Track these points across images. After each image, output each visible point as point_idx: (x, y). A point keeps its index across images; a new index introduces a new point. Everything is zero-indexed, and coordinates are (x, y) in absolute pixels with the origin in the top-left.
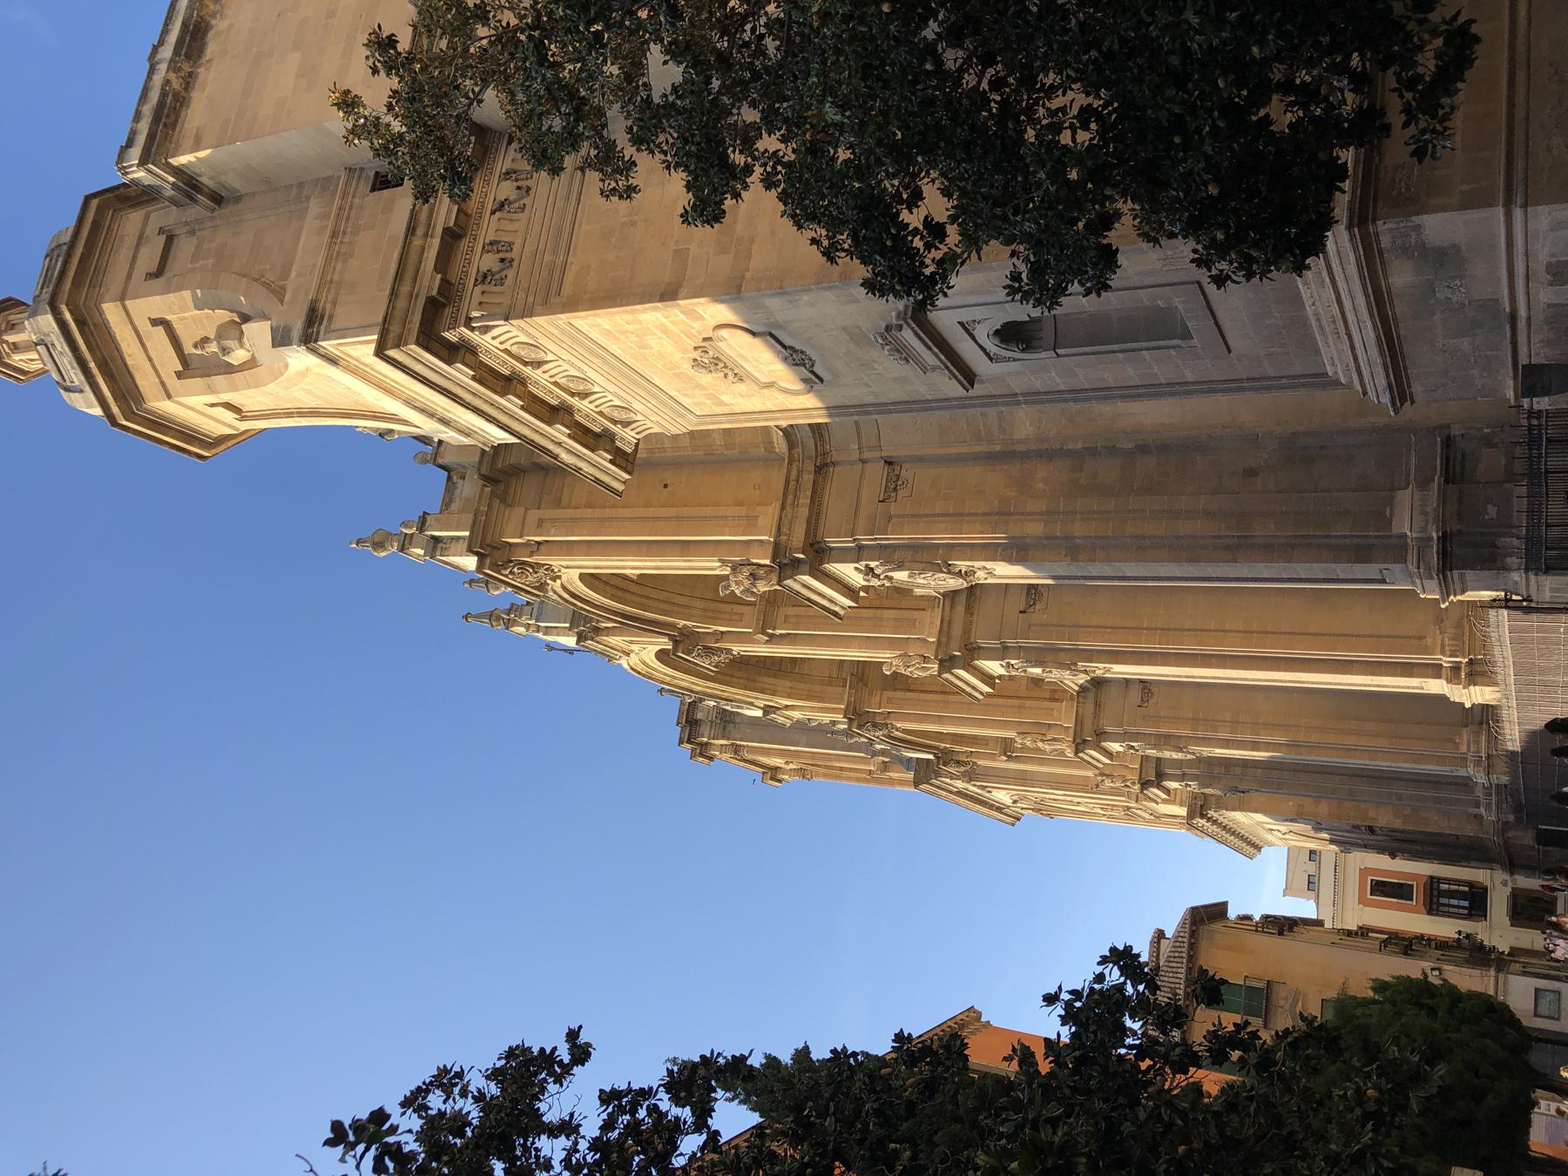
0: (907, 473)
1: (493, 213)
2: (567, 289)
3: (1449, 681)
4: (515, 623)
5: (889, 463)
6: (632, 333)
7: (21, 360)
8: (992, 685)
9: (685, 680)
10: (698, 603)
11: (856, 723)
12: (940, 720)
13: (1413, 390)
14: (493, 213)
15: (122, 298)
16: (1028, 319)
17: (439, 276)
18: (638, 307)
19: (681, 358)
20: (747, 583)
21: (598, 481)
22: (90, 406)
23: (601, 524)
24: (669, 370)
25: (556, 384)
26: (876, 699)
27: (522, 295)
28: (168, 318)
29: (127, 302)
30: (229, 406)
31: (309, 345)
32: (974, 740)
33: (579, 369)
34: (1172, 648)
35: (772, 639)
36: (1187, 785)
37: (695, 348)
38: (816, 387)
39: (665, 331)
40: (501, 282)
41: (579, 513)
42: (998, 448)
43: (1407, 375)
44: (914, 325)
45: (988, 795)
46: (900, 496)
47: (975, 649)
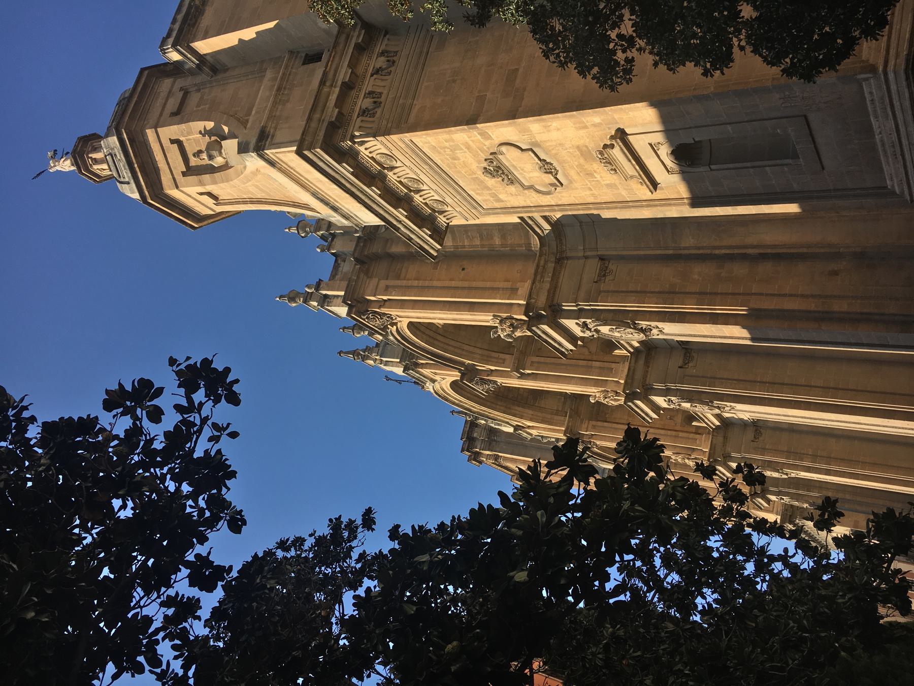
1: (372, 75)
2: (412, 119)
4: (368, 358)
5: (602, 259)
6: (448, 148)
7: (98, 169)
9: (468, 404)
10: (478, 351)
14: (372, 75)
15: (156, 127)
16: (693, 142)
17: (337, 110)
18: (453, 128)
19: (476, 165)
21: (421, 248)
22: (133, 192)
23: (422, 290)
24: (470, 175)
25: (400, 182)
26: (584, 426)
27: (385, 122)
28: (182, 139)
29: (159, 129)
30: (210, 194)
31: (259, 153)
33: (415, 173)
34: (775, 396)
35: (523, 376)
36: (781, 499)
37: (486, 160)
39: (468, 147)
40: (373, 115)
41: (410, 283)
42: (671, 252)
44: (621, 144)
46: (607, 280)
47: (649, 389)
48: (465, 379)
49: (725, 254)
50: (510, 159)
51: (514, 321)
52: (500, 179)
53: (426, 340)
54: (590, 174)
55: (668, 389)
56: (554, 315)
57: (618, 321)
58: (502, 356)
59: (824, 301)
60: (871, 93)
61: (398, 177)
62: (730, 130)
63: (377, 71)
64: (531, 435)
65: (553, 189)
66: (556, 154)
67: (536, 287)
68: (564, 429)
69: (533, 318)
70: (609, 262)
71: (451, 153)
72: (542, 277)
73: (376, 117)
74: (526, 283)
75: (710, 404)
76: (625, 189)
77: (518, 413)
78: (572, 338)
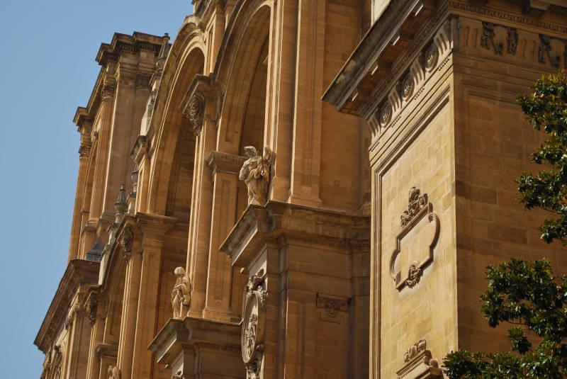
0: (342, 316)
1: (541, 35)
2: (473, 101)
11: (132, 223)
12: (134, 299)
14: (541, 35)
23: (309, 41)
26: (153, 242)
27: (472, 63)
32: (115, 323)
35: (209, 168)
38: (395, 283)
40: (485, 44)
52: (407, 209)
53: (253, 28)
54: (406, 326)
57: (265, 328)
61: (413, 69)
64: (139, 162)
65: (395, 276)
67: (308, 214)
68: (148, 212)
72: (324, 223)
73: (482, 48)
74: (318, 197)
77: (168, 142)
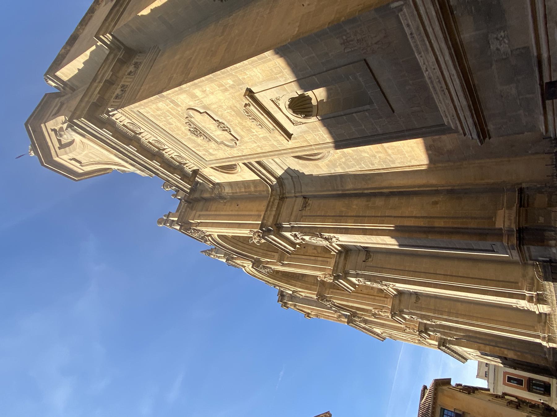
3: (529, 302)
8: (355, 288)
11: (320, 299)
12: (347, 301)
13: (489, 128)
20: (257, 238)
26: (327, 292)
29: (46, 124)
33: (157, 138)
35: (283, 265)
36: (436, 334)
42: (340, 192)
43: (483, 116)
45: (372, 330)
46: (307, 209)
47: (347, 273)
48: (254, 266)
49: (370, 192)
50: (199, 122)
51: (260, 234)
52: (202, 138)
55: (358, 274)
56: (278, 229)
58: (273, 254)
59: (429, 220)
60: (408, 25)
62: (317, 80)
63: (129, 74)
64: (302, 295)
66: (222, 115)
69: (266, 231)
70: (308, 199)
71: (165, 119)
72: (272, 207)
75: (380, 283)
76: (275, 141)
78: (293, 244)
